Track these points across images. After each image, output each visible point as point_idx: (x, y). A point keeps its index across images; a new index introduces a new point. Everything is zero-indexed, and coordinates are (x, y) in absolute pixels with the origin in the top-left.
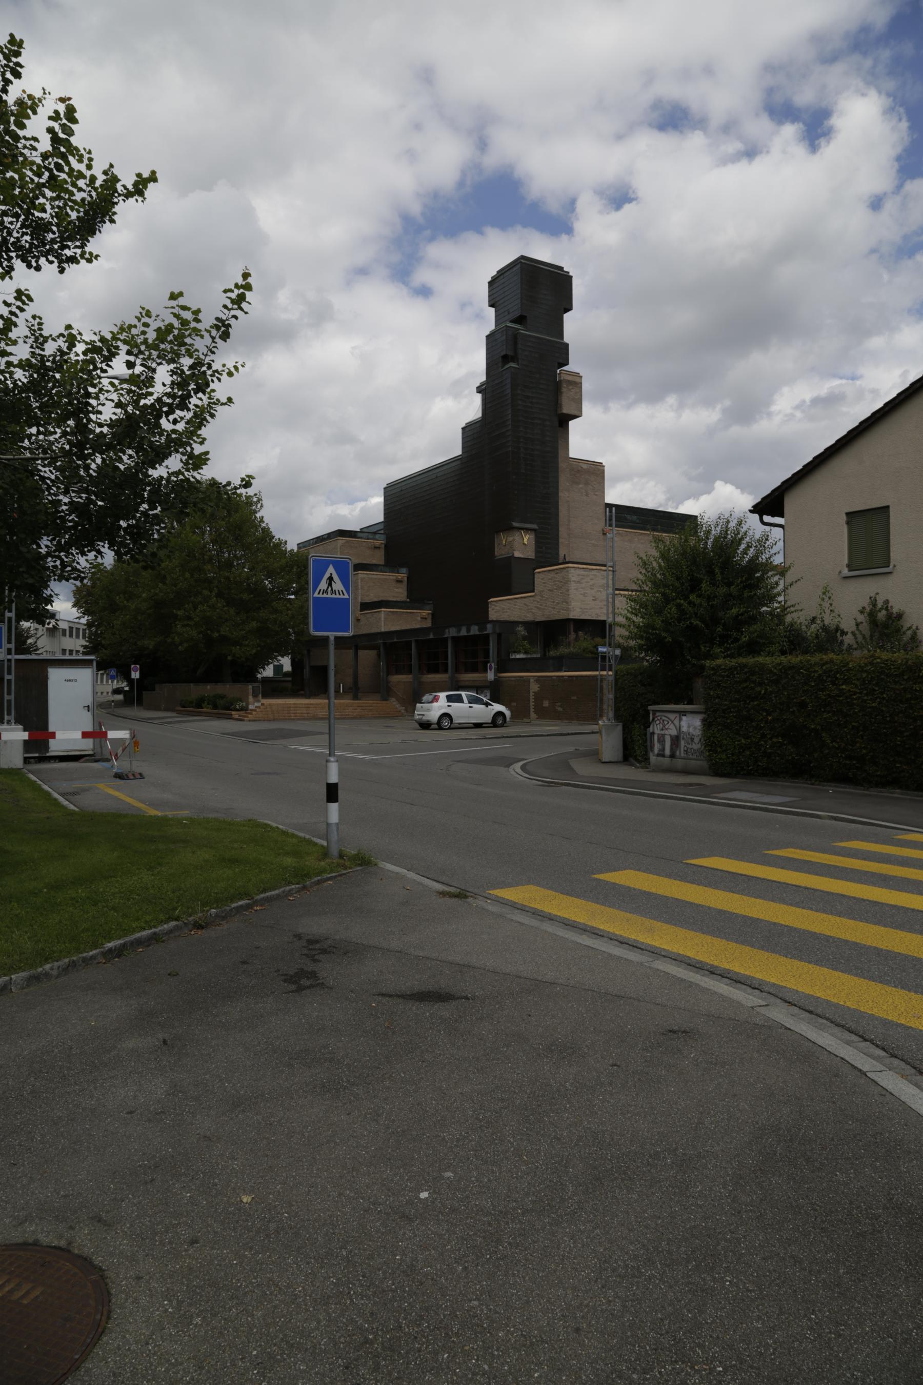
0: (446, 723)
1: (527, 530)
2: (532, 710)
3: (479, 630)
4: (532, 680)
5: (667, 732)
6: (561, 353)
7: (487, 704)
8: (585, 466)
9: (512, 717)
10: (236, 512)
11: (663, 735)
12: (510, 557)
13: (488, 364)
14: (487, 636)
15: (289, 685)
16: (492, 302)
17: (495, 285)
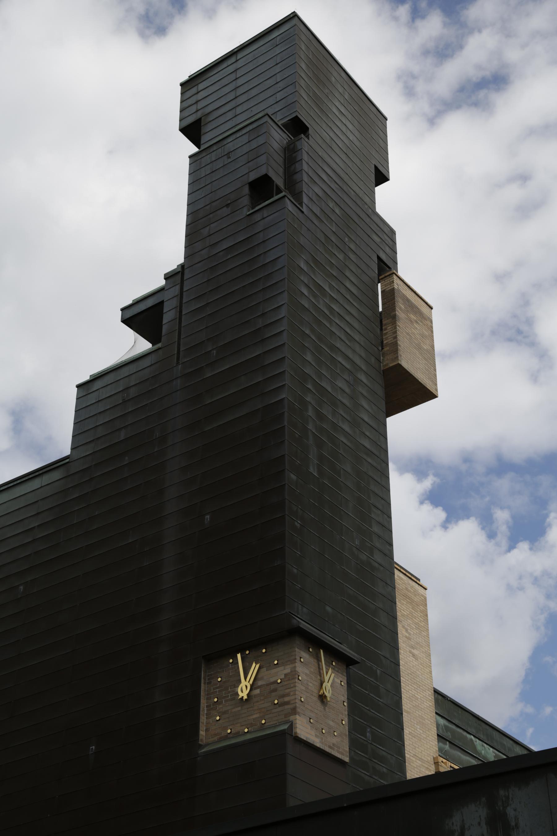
12: (283, 732)
17: (201, 86)
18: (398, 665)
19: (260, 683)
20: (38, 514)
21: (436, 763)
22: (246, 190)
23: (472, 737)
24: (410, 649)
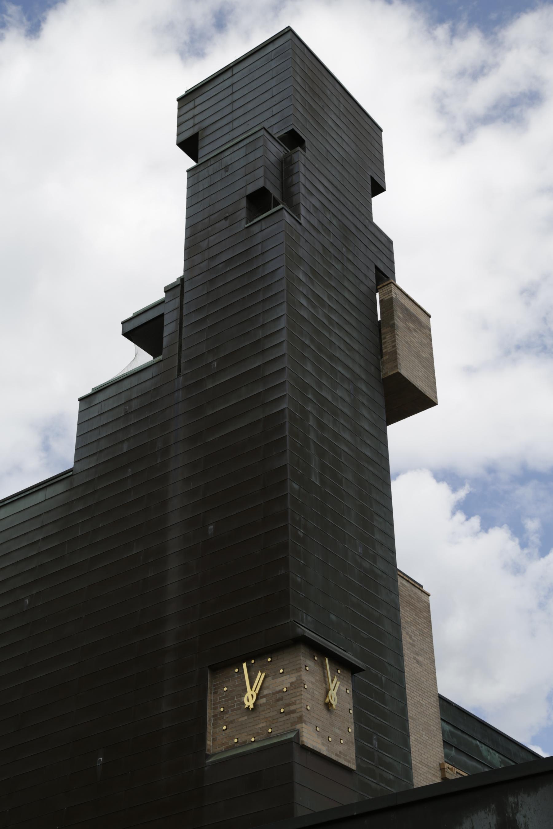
12: (290, 741)
17: (198, 101)
18: (403, 672)
19: (266, 692)
20: (42, 527)
21: (442, 769)
22: (244, 203)
23: (478, 742)
24: (415, 656)
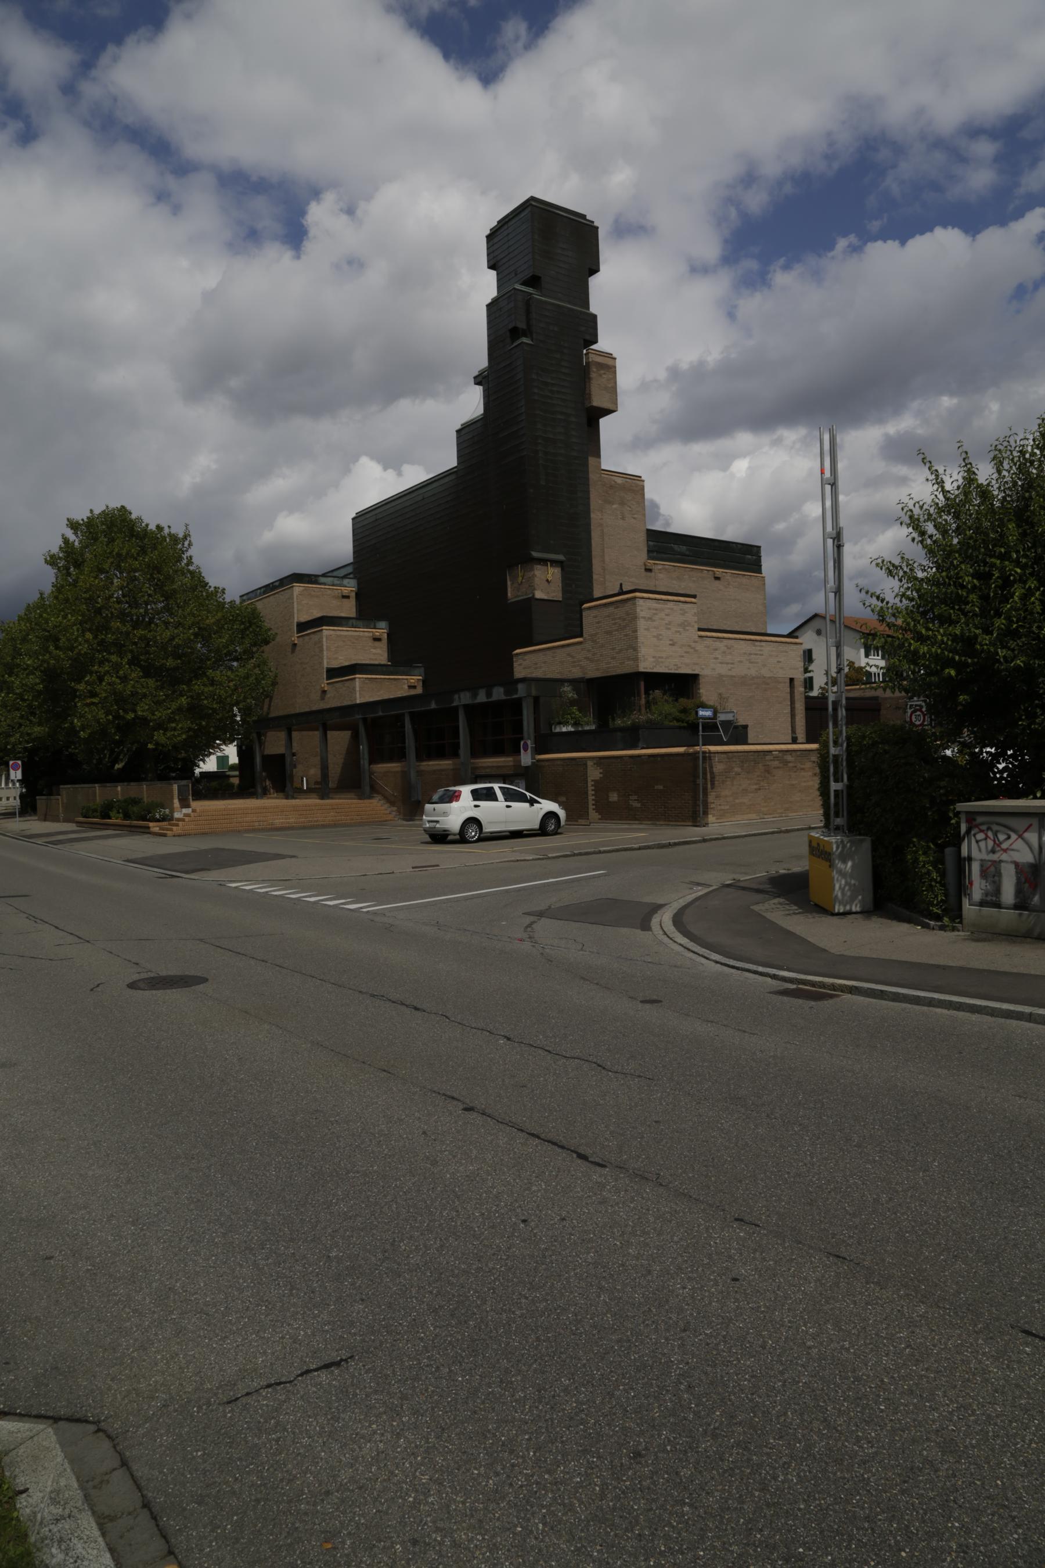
0: (472, 833)
1: (554, 563)
2: (591, 807)
3: (506, 693)
4: (590, 763)
5: (1004, 857)
6: (586, 328)
7: (532, 802)
8: (619, 481)
9: (568, 818)
10: (155, 548)
11: (997, 864)
12: (529, 599)
13: (489, 342)
14: (520, 700)
15: (236, 781)
16: (492, 263)
17: (495, 240)
18: (591, 552)
